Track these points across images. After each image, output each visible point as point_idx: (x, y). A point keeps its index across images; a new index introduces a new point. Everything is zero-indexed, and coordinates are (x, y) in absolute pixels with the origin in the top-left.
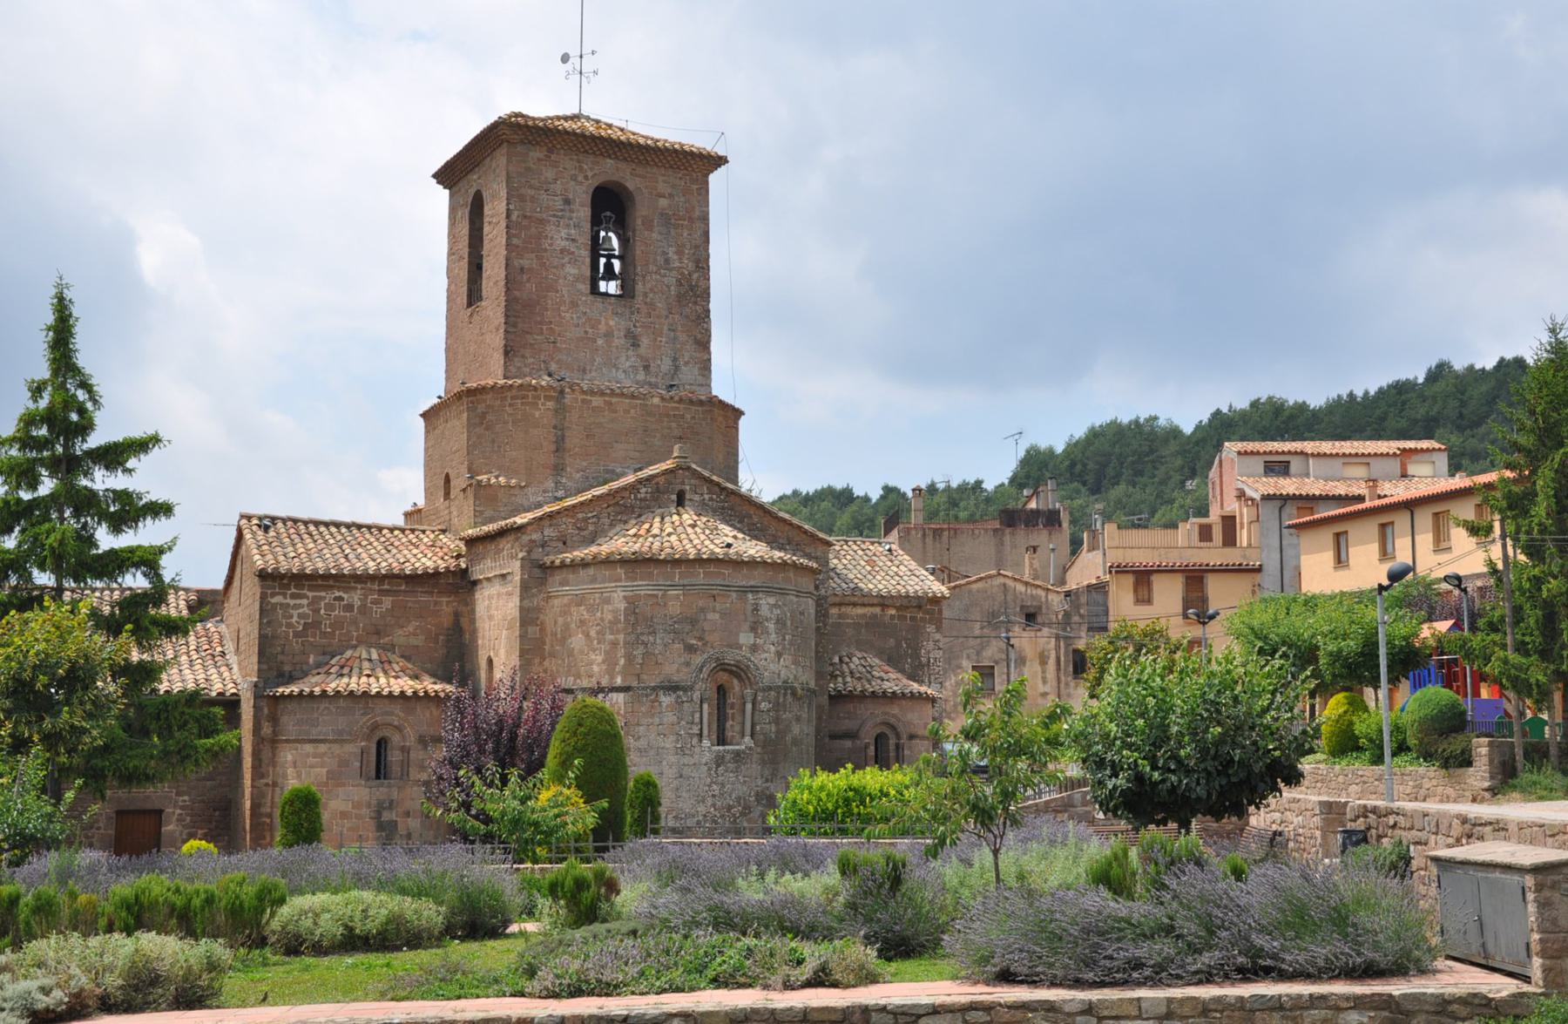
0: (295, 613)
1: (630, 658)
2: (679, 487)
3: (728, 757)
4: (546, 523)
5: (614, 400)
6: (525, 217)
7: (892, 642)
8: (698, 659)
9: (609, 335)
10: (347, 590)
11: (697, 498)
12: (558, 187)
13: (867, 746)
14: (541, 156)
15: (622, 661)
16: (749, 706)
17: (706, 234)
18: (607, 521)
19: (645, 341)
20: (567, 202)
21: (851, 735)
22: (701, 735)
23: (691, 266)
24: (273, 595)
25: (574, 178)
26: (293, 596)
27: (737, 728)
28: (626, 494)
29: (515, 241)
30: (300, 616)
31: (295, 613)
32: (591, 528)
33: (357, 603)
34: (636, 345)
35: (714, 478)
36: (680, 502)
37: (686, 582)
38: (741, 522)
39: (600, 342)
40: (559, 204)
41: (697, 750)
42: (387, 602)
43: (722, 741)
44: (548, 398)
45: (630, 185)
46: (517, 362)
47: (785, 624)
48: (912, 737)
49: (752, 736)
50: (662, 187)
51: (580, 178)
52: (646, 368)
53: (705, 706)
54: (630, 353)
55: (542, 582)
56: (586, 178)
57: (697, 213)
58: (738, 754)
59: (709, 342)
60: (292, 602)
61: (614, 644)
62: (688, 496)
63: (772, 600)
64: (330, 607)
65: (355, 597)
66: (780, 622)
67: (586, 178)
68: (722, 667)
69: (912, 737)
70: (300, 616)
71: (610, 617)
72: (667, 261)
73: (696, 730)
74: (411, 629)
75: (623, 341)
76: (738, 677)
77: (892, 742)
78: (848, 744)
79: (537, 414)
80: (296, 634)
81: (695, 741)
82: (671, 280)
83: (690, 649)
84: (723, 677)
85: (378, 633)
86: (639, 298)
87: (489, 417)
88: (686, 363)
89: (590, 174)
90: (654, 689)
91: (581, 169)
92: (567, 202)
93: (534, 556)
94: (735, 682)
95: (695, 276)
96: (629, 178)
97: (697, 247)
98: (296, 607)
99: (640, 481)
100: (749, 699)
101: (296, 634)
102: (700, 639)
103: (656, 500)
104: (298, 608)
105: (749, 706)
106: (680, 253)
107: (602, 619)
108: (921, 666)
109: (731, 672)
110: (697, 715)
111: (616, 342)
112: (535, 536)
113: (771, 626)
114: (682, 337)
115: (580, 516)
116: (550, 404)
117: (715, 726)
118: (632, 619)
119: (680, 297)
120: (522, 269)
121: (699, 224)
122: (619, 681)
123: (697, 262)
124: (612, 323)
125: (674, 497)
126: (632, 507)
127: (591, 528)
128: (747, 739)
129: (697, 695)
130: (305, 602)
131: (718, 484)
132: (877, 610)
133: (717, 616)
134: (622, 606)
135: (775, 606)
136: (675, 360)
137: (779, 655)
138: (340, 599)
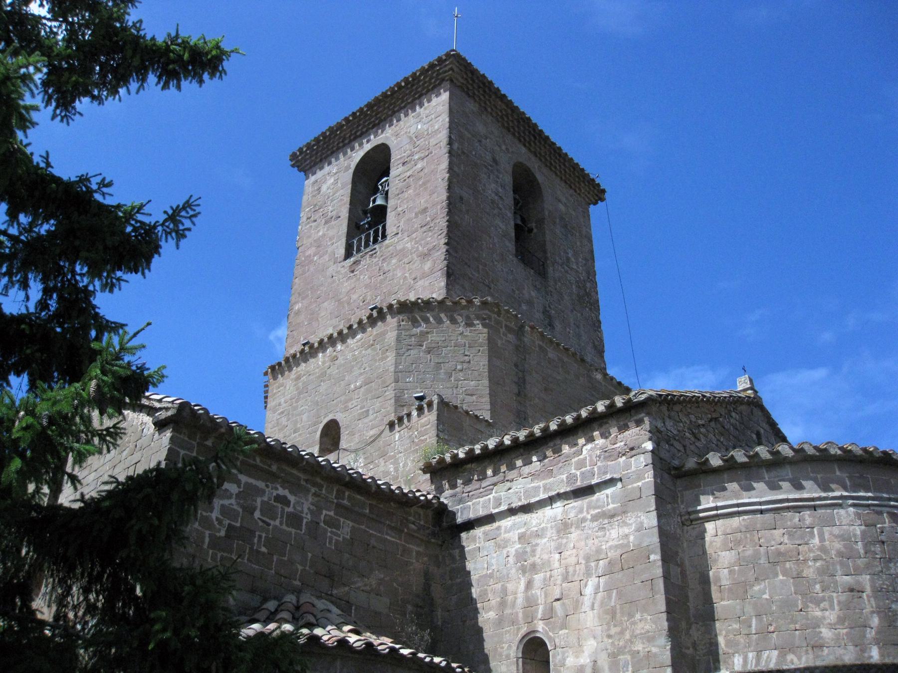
6: (463, 153)
10: (295, 487)
17: (592, 252)
33: (307, 518)
40: (489, 158)
42: (347, 527)
45: (540, 178)
51: (504, 147)
64: (268, 511)
65: (303, 505)
71: (838, 545)
72: (568, 259)
75: (542, 317)
79: (499, 343)
80: (215, 543)
85: (330, 576)
95: (588, 285)
101: (215, 543)
107: (823, 549)
116: (511, 337)
120: (461, 198)
123: (588, 273)
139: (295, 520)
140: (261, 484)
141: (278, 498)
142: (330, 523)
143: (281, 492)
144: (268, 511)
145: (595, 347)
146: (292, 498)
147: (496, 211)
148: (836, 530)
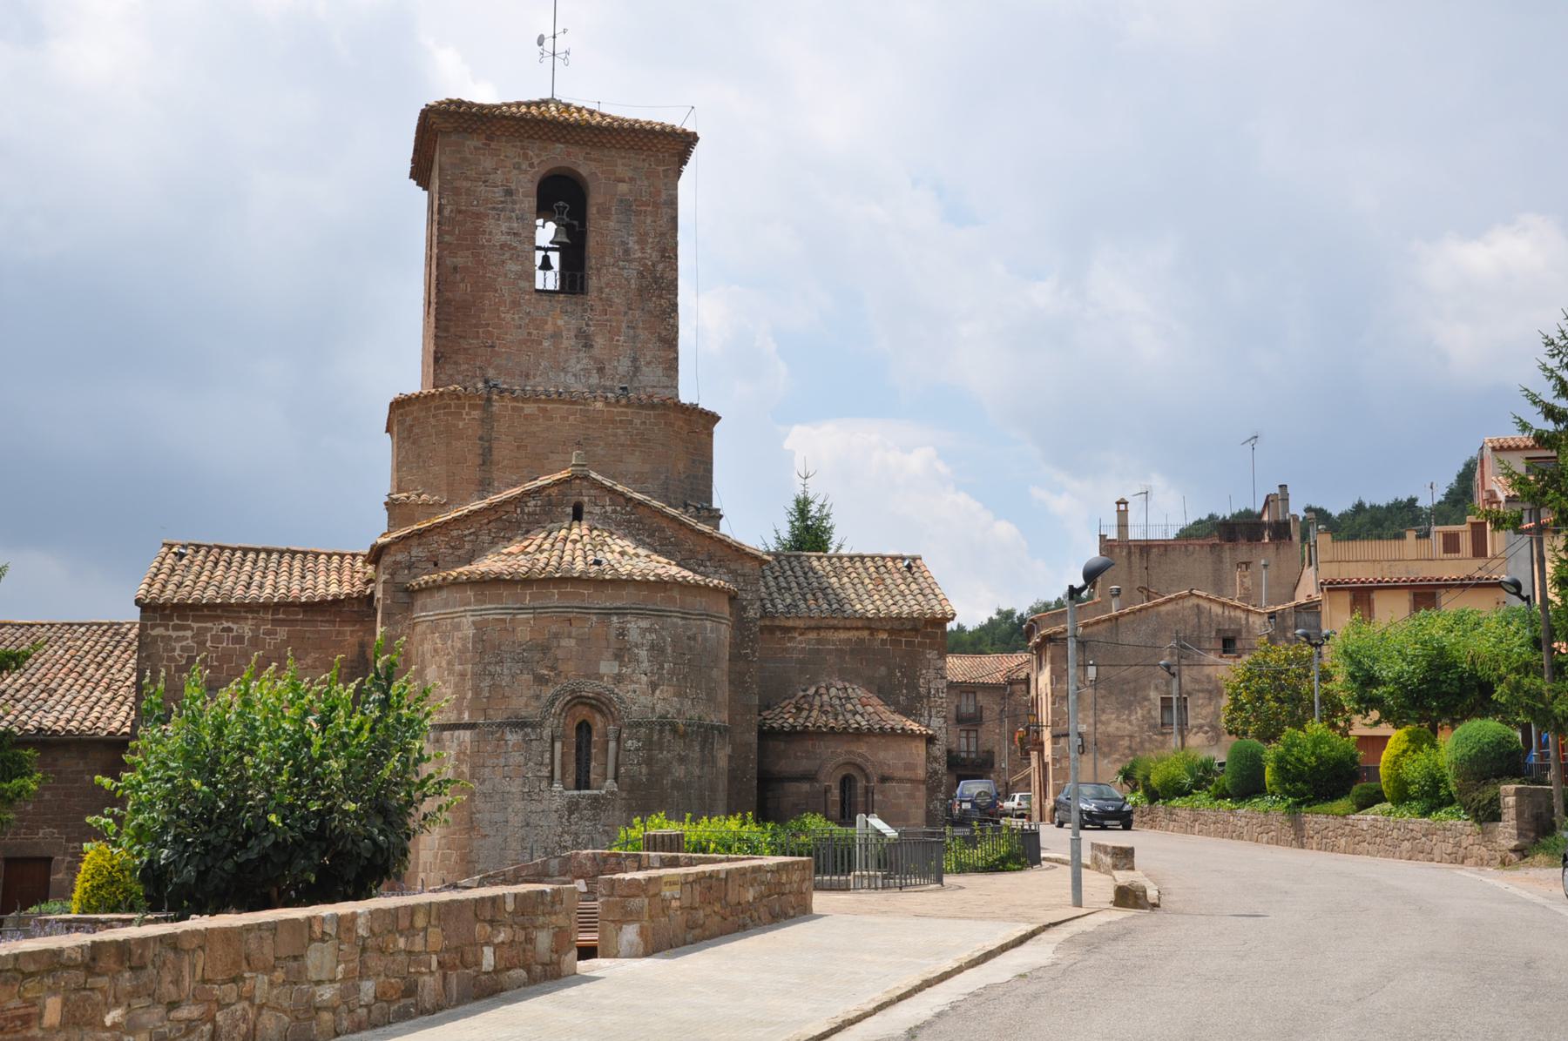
0: (178, 646)
1: (477, 691)
2: (574, 499)
3: (584, 803)
4: (415, 542)
5: (549, 406)
6: (460, 212)
7: (883, 670)
8: (548, 692)
9: (556, 336)
10: (236, 620)
11: (597, 510)
12: (499, 177)
13: (827, 790)
14: (479, 144)
15: (469, 695)
16: (612, 745)
17: (674, 219)
18: (487, 539)
19: (599, 341)
20: (509, 192)
21: (810, 777)
22: (551, 778)
23: (655, 256)
24: (153, 627)
25: (517, 167)
26: (176, 628)
27: (599, 770)
28: (511, 508)
29: (447, 238)
30: (183, 649)
31: (178, 646)
32: (468, 546)
34: (588, 345)
35: (619, 488)
36: (578, 515)
37: (537, 604)
38: (651, 536)
39: (546, 344)
40: (498, 194)
41: (546, 795)
42: (282, 633)
43: (582, 782)
44: (472, 407)
45: (584, 171)
46: (449, 369)
47: (662, 651)
48: (884, 779)
49: (616, 779)
50: (621, 170)
52: (601, 370)
53: (558, 745)
54: (582, 354)
55: (408, 607)
56: (531, 165)
57: (664, 197)
58: (596, 799)
59: (676, 339)
60: (175, 634)
61: (463, 675)
62: (586, 509)
63: (644, 624)
64: (217, 639)
65: (246, 628)
66: (656, 650)
67: (531, 165)
68: (578, 700)
69: (884, 779)
70: (183, 649)
71: (459, 645)
72: (627, 252)
73: (545, 772)
74: (310, 662)
76: (600, 711)
77: (861, 784)
78: (805, 787)
79: (461, 425)
81: (544, 784)
82: (631, 272)
83: (541, 680)
84: (583, 713)
86: (593, 294)
87: (416, 430)
88: (649, 363)
89: (536, 161)
90: (500, 725)
91: (525, 156)
92: (509, 192)
93: (399, 579)
94: (598, 717)
95: (660, 267)
96: (584, 164)
97: (662, 235)
98: (179, 639)
99: (527, 494)
100: (612, 736)
102: (553, 668)
103: (547, 514)
104: (182, 638)
105: (612, 745)
106: (642, 242)
108: (919, 698)
109: (592, 706)
110: (547, 755)
111: (565, 343)
112: (399, 557)
113: (643, 654)
114: (644, 335)
115: (455, 533)
116: (476, 414)
117: (572, 767)
118: (480, 646)
119: (641, 291)
120: (455, 268)
121: (665, 210)
122: (466, 717)
123: (663, 250)
124: (560, 322)
125: (570, 510)
126: (519, 523)
127: (468, 546)
128: (610, 782)
129: (547, 732)
130: (189, 633)
131: (622, 494)
132: (866, 634)
133: (573, 642)
134: (471, 632)
135: (650, 630)
136: (635, 360)
137: (654, 686)
138: (230, 630)
139: (239, 639)
140: (209, 625)
141: (224, 630)
142: (267, 633)
143: (226, 625)
144: (217, 639)
145: (662, 340)
146: (235, 627)
147: (507, 255)
148: (460, 634)
